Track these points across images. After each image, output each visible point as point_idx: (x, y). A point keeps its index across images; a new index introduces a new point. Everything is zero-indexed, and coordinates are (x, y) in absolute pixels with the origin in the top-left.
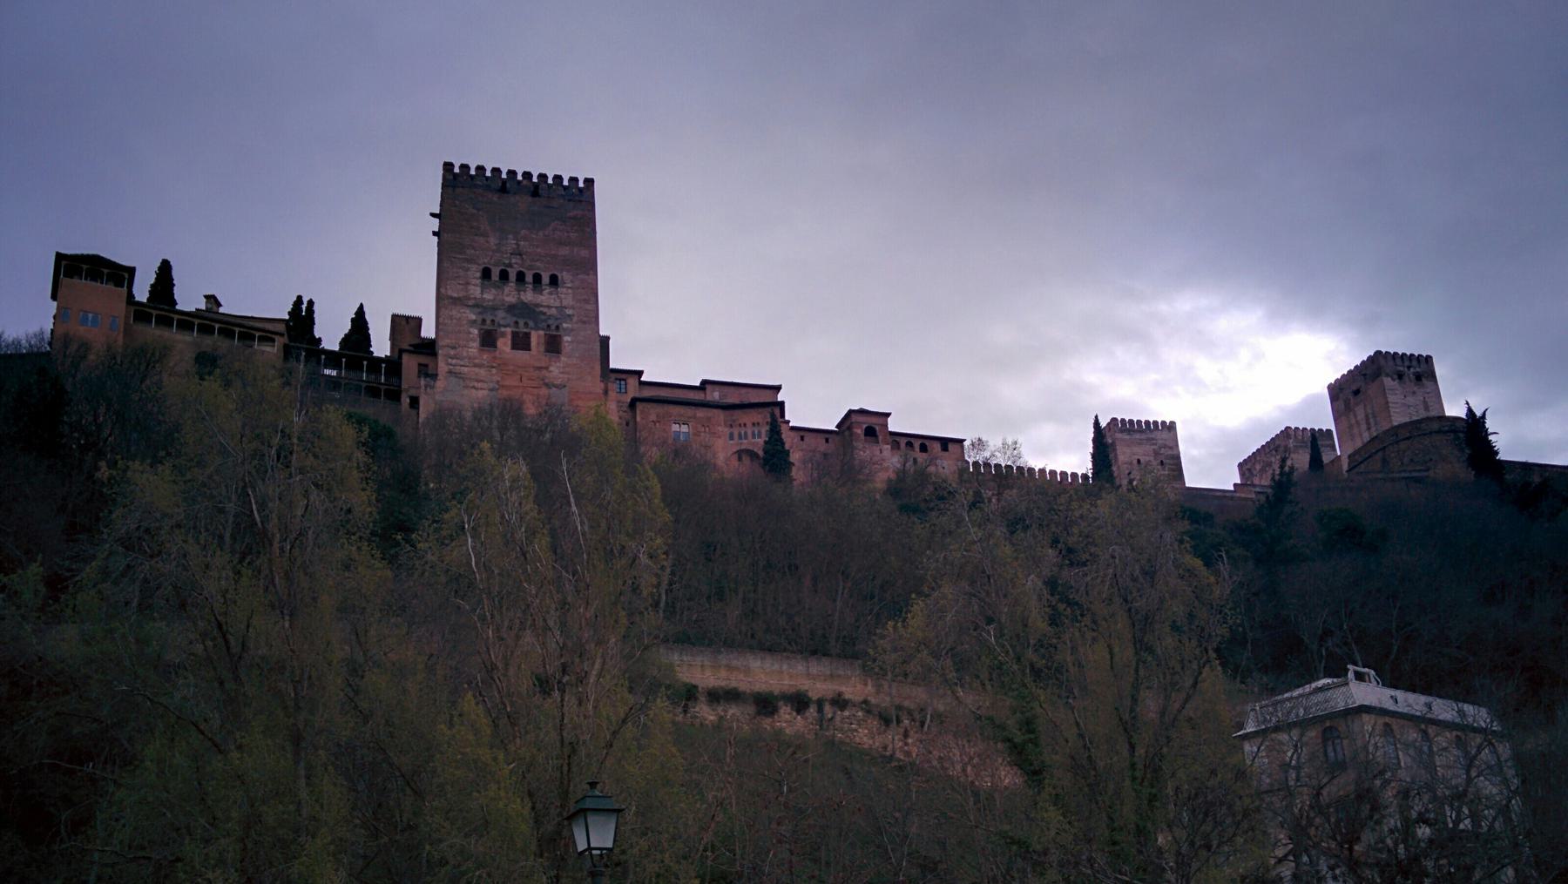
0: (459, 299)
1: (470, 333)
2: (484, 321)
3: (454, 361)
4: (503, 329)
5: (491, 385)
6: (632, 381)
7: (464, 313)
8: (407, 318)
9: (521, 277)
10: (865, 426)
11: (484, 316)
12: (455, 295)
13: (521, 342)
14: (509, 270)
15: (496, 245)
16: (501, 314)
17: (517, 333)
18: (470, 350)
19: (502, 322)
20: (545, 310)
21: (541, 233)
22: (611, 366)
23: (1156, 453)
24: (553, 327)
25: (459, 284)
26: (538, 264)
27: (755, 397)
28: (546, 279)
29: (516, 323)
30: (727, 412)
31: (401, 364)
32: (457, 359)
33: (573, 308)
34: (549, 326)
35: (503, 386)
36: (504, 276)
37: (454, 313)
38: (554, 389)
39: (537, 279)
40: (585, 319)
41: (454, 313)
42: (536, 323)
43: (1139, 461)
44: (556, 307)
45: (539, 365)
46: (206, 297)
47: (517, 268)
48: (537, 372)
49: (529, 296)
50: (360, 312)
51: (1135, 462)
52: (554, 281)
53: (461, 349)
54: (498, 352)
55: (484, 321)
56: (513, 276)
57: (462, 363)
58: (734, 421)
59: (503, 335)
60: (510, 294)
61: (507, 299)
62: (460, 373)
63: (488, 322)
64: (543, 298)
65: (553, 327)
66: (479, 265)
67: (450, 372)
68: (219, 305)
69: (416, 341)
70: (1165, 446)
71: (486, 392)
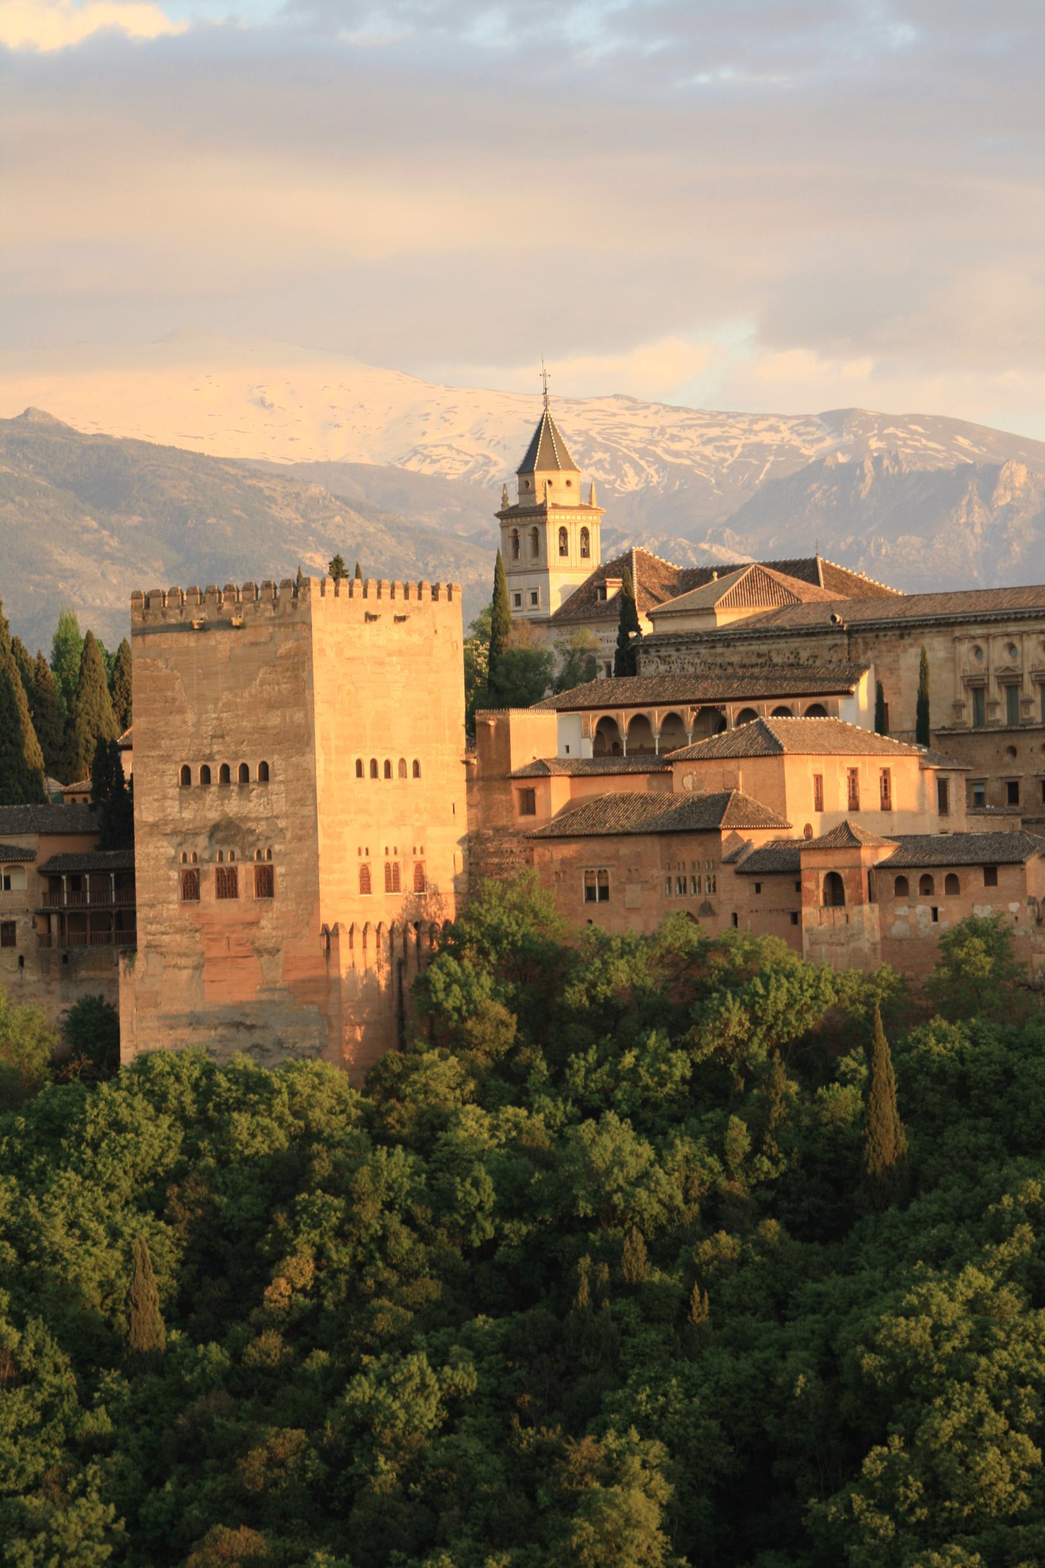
0: (154, 826)
1: (169, 879)
2: (185, 855)
3: (153, 928)
9: (225, 770)
10: (822, 875)
12: (151, 819)
13: (227, 887)
14: (210, 765)
15: (194, 725)
16: (202, 841)
18: (171, 906)
19: (206, 855)
20: (252, 825)
21: (246, 695)
24: (265, 854)
26: (244, 747)
28: (254, 774)
29: (221, 853)
32: (158, 923)
33: (286, 816)
34: (259, 852)
35: (209, 960)
38: (266, 956)
39: (244, 769)
41: (151, 849)
44: (267, 818)
49: (234, 806)
55: (185, 855)
57: (163, 929)
62: (160, 946)
63: (190, 858)
64: (251, 805)
65: (265, 854)
66: (176, 762)
67: (149, 946)
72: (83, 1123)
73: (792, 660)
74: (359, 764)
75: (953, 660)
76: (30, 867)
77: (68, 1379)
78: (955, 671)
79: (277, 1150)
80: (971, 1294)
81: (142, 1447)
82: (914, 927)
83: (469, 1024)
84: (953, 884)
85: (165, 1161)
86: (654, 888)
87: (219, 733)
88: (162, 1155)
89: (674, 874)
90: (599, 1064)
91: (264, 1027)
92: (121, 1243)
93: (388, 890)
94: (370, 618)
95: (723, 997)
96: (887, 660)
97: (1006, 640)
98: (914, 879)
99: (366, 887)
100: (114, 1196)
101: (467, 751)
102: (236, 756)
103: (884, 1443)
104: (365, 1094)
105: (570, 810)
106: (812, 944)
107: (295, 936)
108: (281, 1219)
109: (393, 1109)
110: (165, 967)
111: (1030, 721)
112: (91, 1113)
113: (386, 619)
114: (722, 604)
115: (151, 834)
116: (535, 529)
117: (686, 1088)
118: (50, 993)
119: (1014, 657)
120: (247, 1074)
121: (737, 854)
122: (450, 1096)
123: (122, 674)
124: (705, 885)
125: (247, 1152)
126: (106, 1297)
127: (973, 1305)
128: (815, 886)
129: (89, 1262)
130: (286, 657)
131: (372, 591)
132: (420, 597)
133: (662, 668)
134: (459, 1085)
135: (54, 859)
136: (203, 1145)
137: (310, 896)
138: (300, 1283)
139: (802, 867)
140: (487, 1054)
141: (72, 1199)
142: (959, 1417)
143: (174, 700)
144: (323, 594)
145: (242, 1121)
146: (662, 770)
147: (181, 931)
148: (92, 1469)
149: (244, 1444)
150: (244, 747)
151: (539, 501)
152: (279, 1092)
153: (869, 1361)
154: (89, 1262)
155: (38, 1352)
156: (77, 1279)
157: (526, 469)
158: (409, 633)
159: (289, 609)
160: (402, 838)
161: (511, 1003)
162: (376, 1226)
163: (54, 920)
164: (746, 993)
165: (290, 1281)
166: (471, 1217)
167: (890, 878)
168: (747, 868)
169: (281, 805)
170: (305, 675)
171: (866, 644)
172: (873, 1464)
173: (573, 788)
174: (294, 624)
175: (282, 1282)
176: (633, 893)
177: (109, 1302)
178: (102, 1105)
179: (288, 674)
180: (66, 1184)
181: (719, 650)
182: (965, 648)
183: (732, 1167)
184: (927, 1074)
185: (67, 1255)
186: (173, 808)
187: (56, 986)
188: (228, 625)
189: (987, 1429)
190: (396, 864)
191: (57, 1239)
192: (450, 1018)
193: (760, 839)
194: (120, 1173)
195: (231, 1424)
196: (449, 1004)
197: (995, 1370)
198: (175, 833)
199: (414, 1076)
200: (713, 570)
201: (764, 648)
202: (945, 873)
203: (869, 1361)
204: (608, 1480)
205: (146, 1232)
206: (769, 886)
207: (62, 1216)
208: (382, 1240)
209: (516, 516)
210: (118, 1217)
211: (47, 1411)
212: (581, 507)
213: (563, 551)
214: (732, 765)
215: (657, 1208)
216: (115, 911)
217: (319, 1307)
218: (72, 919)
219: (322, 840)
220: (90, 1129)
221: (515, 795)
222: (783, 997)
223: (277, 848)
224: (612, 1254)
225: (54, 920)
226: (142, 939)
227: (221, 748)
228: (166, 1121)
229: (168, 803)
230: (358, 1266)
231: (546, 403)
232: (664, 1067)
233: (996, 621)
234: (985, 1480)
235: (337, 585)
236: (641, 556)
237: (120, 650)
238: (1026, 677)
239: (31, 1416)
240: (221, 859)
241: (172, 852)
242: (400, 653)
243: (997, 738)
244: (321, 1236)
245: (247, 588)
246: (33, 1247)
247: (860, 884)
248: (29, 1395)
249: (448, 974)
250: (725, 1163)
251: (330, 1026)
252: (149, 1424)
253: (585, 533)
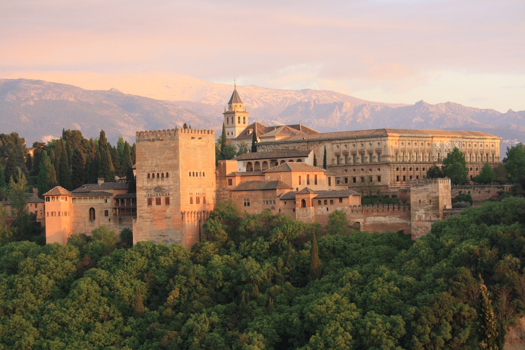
0: (141, 187)
3: (140, 212)
4: (153, 197)
5: (151, 220)
9: (158, 174)
10: (301, 200)
12: (140, 186)
13: (158, 202)
14: (155, 173)
16: (153, 191)
19: (153, 195)
20: (164, 187)
23: (428, 196)
24: (167, 194)
26: (162, 169)
28: (165, 175)
30: (263, 191)
35: (154, 220)
36: (153, 174)
39: (163, 174)
42: (162, 194)
43: (420, 200)
47: (157, 172)
49: (160, 183)
51: (418, 201)
52: (167, 174)
60: (155, 183)
63: (150, 195)
65: (167, 194)
67: (140, 216)
70: (432, 192)
72: (124, 258)
73: (294, 149)
74: (190, 173)
75: (332, 149)
76: (112, 197)
77: (121, 319)
78: (332, 151)
79: (170, 265)
80: (335, 299)
81: (138, 335)
82: (322, 212)
83: (216, 235)
84: (332, 202)
85: (144, 267)
86: (260, 203)
88: (143, 265)
89: (265, 200)
90: (247, 245)
91: (167, 236)
92: (133, 287)
93: (197, 203)
94: (193, 138)
95: (277, 229)
96: (316, 148)
97: (345, 144)
98: (322, 201)
99: (191, 202)
100: (132, 276)
101: (216, 170)
102: (161, 171)
103: (315, 335)
104: (191, 252)
105: (241, 185)
106: (298, 216)
107: (175, 214)
108: (171, 281)
109: (198, 255)
110: (144, 221)
111: (350, 163)
112: (126, 256)
113: (197, 138)
114: (277, 136)
116: (232, 117)
117: (268, 251)
118: (116, 227)
119: (347, 148)
120: (163, 247)
121: (280, 195)
122: (212, 252)
123: (134, 151)
124: (273, 202)
125: (163, 265)
126: (130, 300)
127: (336, 302)
128: (299, 203)
129: (126, 291)
130: (173, 147)
131: (193, 132)
132: (205, 133)
133: (263, 150)
134: (214, 250)
135: (117, 195)
136: (153, 264)
137: (178, 205)
138: (176, 296)
139: (296, 198)
140: (220, 242)
141: (122, 276)
142: (333, 328)
143: (146, 157)
144: (182, 132)
145: (162, 258)
146: (263, 175)
147: (147, 213)
148: (126, 340)
149: (163, 334)
150: (162, 169)
151: (233, 110)
152: (171, 251)
153: (311, 315)
154: (126, 291)
155: (114, 313)
156: (123, 295)
157: (230, 103)
158: (202, 142)
159: (173, 136)
160: (200, 191)
161: (226, 230)
162: (194, 283)
163: (117, 210)
164: (282, 228)
165: (173, 296)
166: (216, 281)
167: (317, 201)
168: (283, 198)
169: (171, 183)
170: (177, 151)
171: (311, 145)
172: (312, 339)
173: (241, 179)
174: (175, 140)
175: (171, 297)
176: (255, 204)
177: (130, 301)
178: (129, 254)
180: (120, 273)
181: (276, 146)
182: (335, 146)
183: (279, 270)
184: (326, 247)
185: (120, 290)
186: (146, 183)
187: (118, 226)
188: (159, 140)
189: (339, 331)
190: (199, 197)
191: (118, 286)
192: (211, 234)
193: (287, 191)
194: (133, 270)
195: (160, 330)
196: (211, 230)
197: (341, 317)
198: (146, 189)
199: (203, 248)
200: (275, 127)
201: (287, 146)
202: (330, 199)
203: (311, 315)
204: (249, 344)
205: (139, 284)
206: (288, 202)
207: (119, 280)
208: (195, 286)
209: (228, 114)
210: (133, 281)
211: (116, 326)
212: (244, 112)
213: (239, 122)
214: (279, 174)
215: (261, 279)
216: (132, 208)
217: (180, 302)
218: (122, 210)
219: (181, 191)
220: (126, 260)
221: (227, 180)
222: (291, 229)
223: (170, 193)
224: (250, 290)
225: (117, 210)
226: (138, 215)
228: (144, 258)
229: (145, 182)
230: (190, 293)
231: (235, 87)
232: (263, 246)
233: (342, 139)
234: (339, 343)
235: (185, 130)
236: (258, 124)
237: (133, 146)
238: (349, 153)
239: (112, 327)
240: (157, 196)
241: (145, 194)
242: (200, 146)
243: (342, 167)
244: (181, 286)
245: (164, 131)
246: (112, 287)
247: (310, 202)
248: (112, 323)
249: (211, 223)
250: (277, 269)
251: (183, 235)
252: (140, 330)
253: (244, 118)
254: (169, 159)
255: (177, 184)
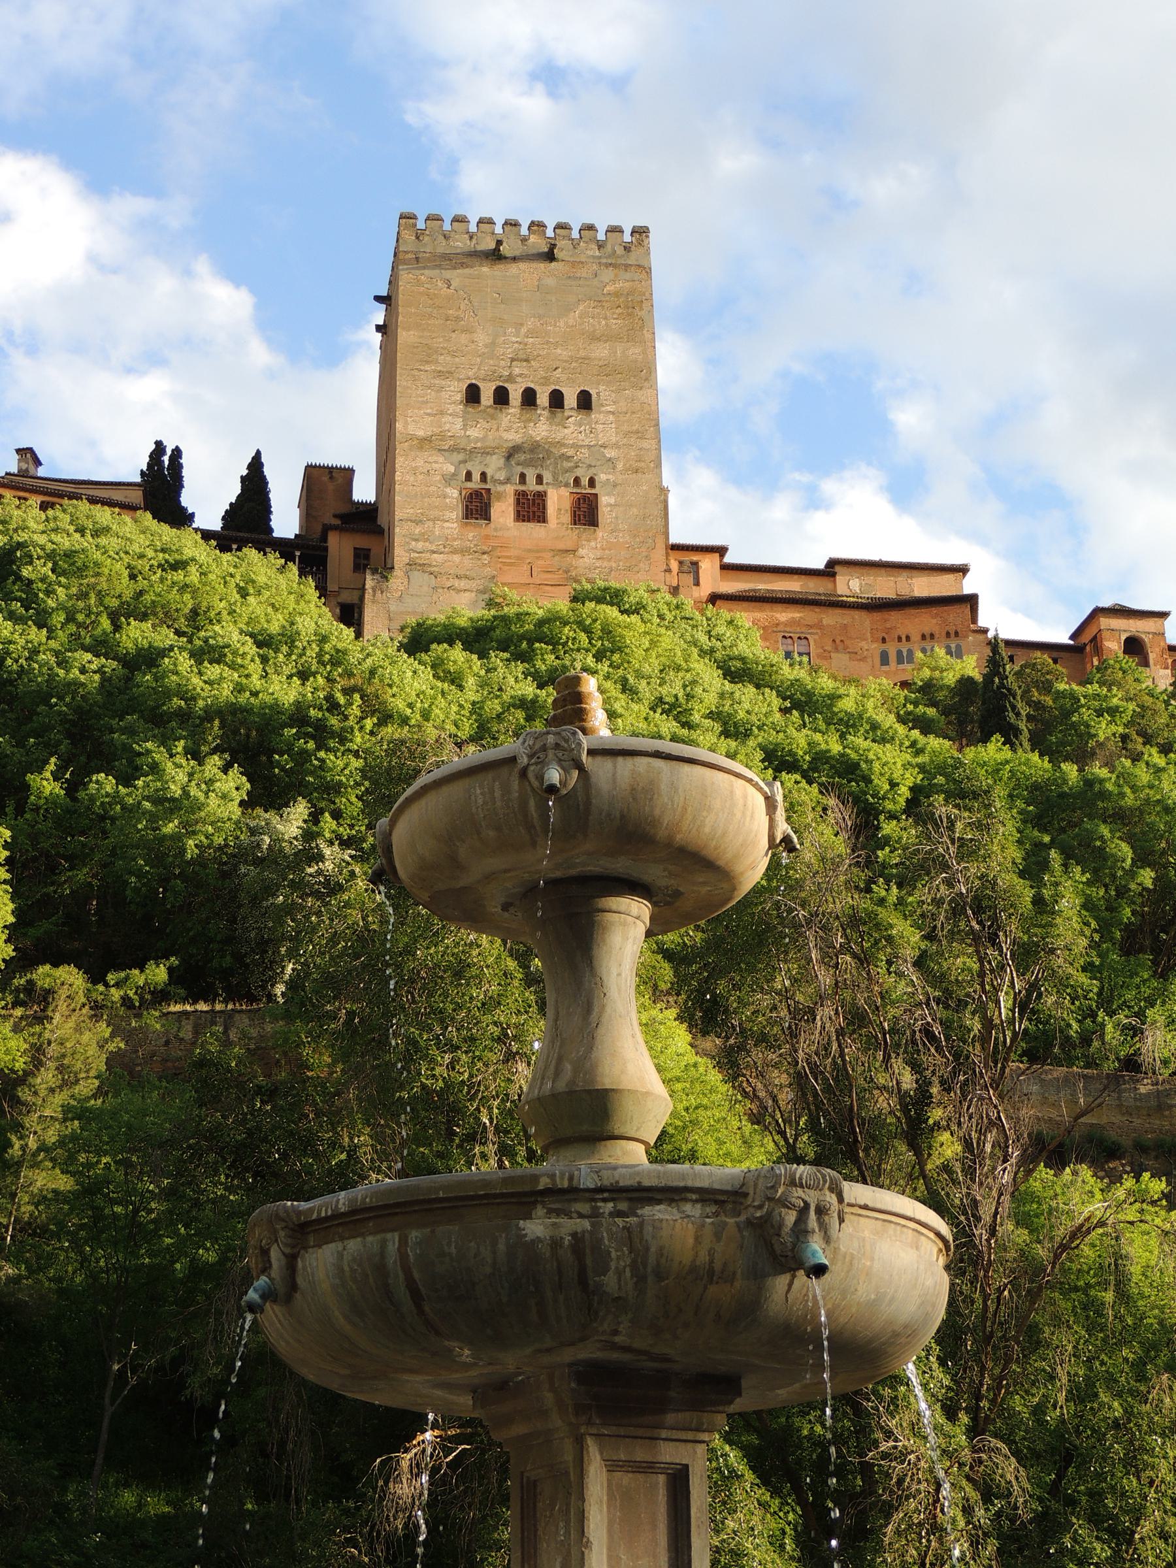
3: (420, 545)
4: (500, 488)
6: (708, 566)
7: (436, 462)
8: (331, 471)
9: (529, 398)
10: (1123, 638)
11: (469, 466)
12: (421, 433)
15: (486, 346)
17: (524, 493)
18: (447, 525)
20: (571, 452)
21: (562, 324)
22: (674, 540)
24: (585, 481)
25: (428, 414)
27: (922, 587)
28: (571, 400)
29: (523, 477)
30: (877, 616)
31: (326, 549)
32: (426, 540)
33: (616, 446)
34: (577, 481)
36: (501, 396)
37: (420, 462)
39: (557, 400)
40: (639, 464)
41: (420, 462)
44: (589, 447)
45: (562, 546)
46: (18, 451)
48: (557, 558)
50: (256, 465)
52: (585, 402)
53: (431, 523)
54: (492, 525)
55: (469, 476)
56: (515, 396)
57: (434, 548)
58: (888, 631)
59: (500, 496)
61: (506, 436)
62: (430, 565)
63: (476, 476)
64: (566, 431)
65: (585, 481)
66: (459, 380)
67: (411, 564)
68: (38, 463)
69: (344, 509)
71: (473, 594)
87: (524, 357)
102: (546, 381)
115: (421, 448)
130: (617, 294)
147: (463, 551)
159: (620, 251)
174: (627, 267)
179: (619, 311)
223: (602, 477)
226: (400, 556)
227: (525, 372)
254: (594, 338)
255: (645, 444)
